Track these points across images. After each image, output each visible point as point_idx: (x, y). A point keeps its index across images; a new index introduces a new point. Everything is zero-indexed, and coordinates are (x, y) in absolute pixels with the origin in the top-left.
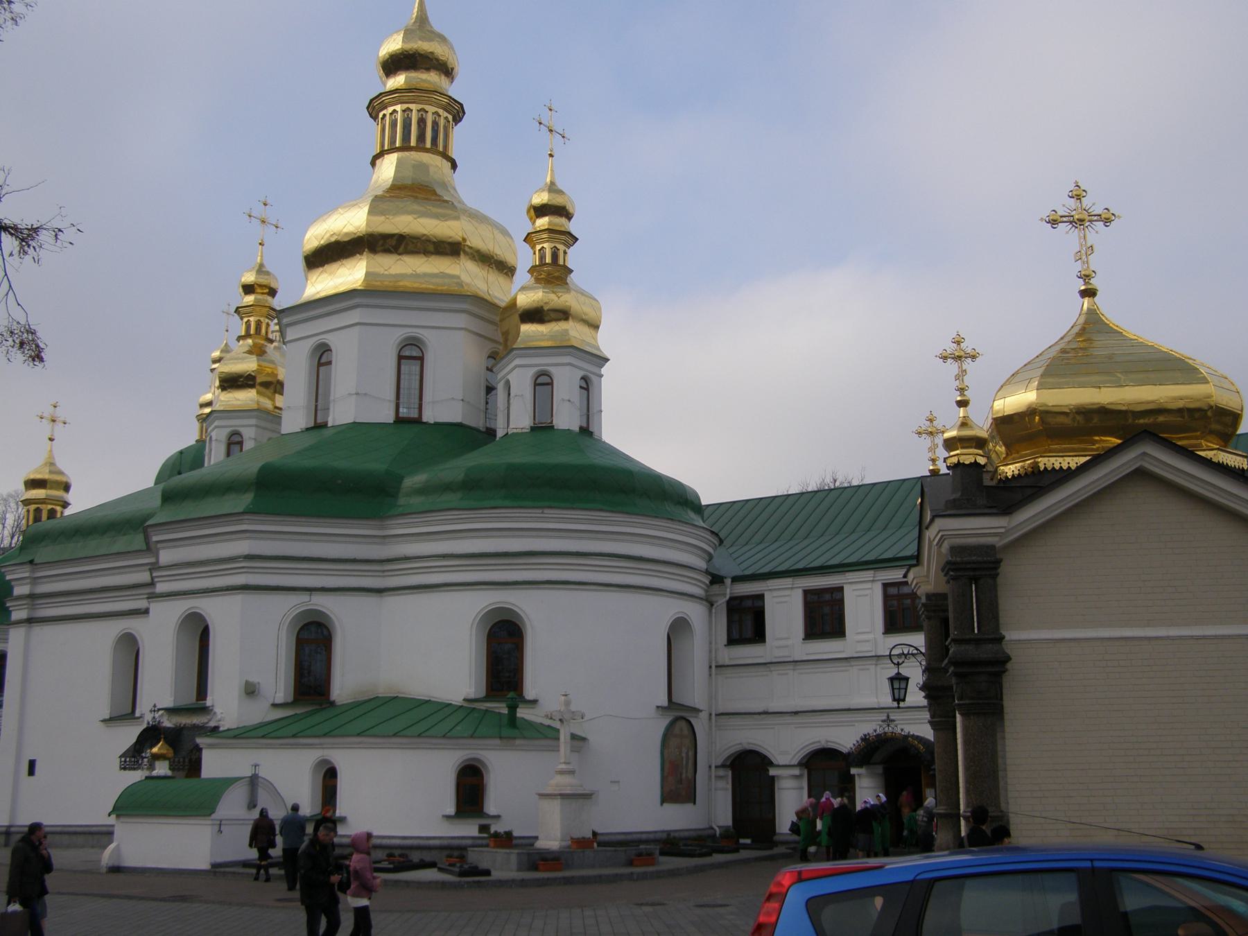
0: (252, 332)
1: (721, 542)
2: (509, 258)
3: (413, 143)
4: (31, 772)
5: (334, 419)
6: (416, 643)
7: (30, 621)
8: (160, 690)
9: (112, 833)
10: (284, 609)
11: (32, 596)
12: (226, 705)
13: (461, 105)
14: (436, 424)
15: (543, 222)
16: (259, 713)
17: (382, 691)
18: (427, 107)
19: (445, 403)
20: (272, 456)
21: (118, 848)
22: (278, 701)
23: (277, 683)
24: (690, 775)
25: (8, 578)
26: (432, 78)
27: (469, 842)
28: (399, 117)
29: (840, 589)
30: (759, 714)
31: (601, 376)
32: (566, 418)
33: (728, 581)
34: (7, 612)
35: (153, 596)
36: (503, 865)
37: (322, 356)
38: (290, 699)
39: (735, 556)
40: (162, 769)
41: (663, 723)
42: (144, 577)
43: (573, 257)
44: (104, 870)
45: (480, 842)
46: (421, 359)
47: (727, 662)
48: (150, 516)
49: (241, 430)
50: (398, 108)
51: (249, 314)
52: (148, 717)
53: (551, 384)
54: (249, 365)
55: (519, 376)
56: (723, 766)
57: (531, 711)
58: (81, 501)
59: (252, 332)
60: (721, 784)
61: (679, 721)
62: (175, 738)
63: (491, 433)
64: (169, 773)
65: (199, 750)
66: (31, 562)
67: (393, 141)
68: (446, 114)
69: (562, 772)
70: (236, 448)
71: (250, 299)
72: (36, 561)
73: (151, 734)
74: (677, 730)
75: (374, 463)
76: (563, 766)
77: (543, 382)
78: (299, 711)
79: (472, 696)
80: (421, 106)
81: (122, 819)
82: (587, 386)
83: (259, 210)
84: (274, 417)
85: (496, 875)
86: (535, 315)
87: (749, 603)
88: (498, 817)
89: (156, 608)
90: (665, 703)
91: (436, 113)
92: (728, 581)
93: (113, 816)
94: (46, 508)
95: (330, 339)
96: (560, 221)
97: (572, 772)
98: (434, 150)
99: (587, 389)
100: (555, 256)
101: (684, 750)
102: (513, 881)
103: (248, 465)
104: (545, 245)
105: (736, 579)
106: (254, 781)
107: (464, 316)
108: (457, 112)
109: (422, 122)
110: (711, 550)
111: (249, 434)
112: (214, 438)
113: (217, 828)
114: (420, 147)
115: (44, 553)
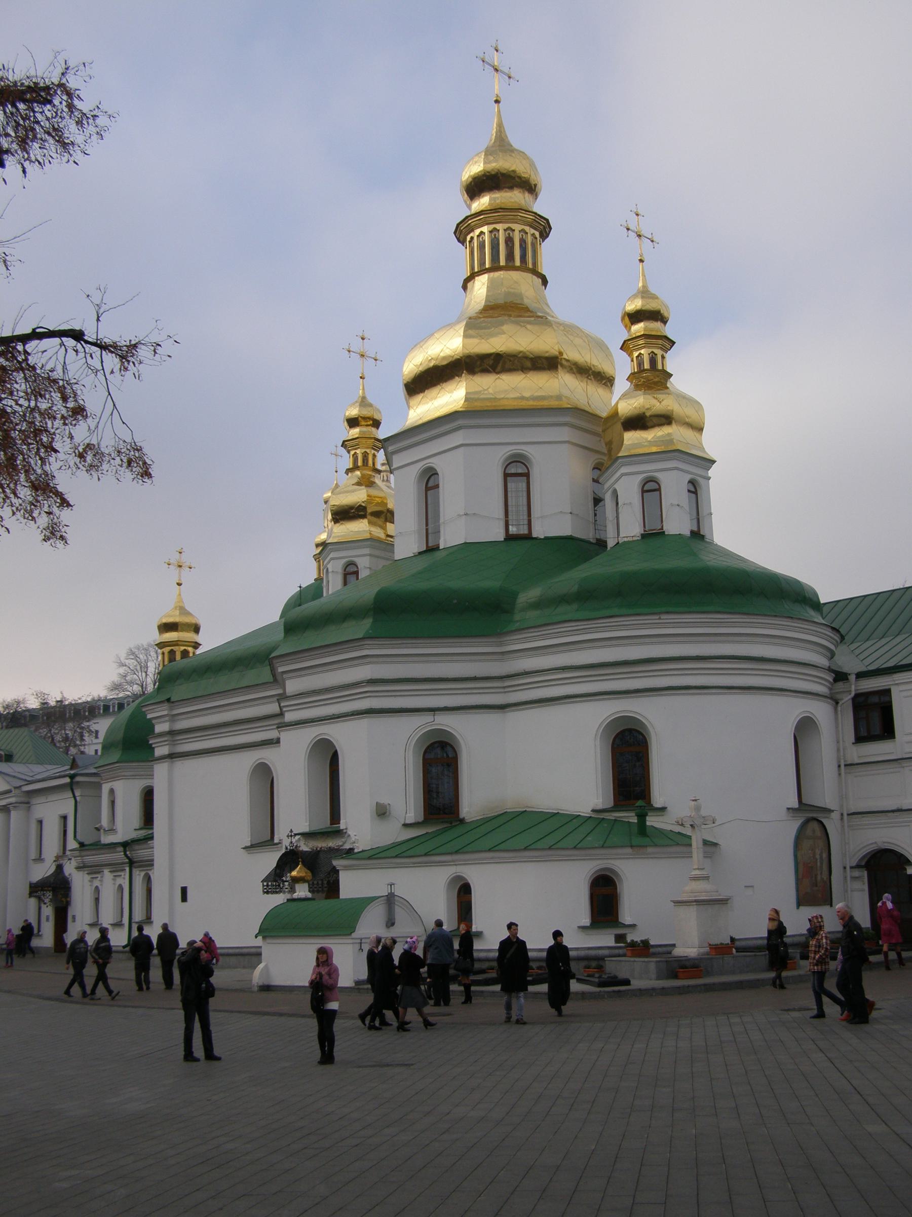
0: (360, 463)
1: (842, 638)
2: (606, 368)
3: (502, 262)
4: (184, 898)
5: (445, 541)
6: (539, 757)
7: (172, 756)
8: (295, 816)
9: (260, 954)
11: (172, 733)
12: (360, 828)
13: (547, 220)
14: (546, 538)
15: (639, 328)
16: (391, 833)
17: (511, 805)
18: (513, 226)
19: (554, 517)
20: (387, 582)
21: (266, 966)
22: (408, 822)
23: (407, 804)
24: (825, 878)
25: (149, 716)
26: (514, 197)
27: (606, 952)
28: (487, 238)
30: (893, 811)
31: (709, 478)
32: (677, 523)
33: (852, 678)
34: (151, 749)
35: (280, 726)
36: (642, 975)
37: (429, 481)
38: (421, 818)
39: (857, 652)
40: (302, 891)
41: (795, 825)
42: (273, 708)
43: (672, 362)
44: (256, 989)
45: (617, 951)
46: (527, 475)
47: (857, 761)
48: (274, 649)
50: (485, 229)
51: (355, 447)
52: (286, 842)
53: (659, 490)
54: (359, 496)
55: (626, 485)
56: (858, 866)
57: (661, 819)
58: (210, 640)
59: (360, 463)
60: (857, 885)
61: (811, 822)
62: (312, 861)
63: (601, 544)
64: (309, 895)
65: (336, 872)
66: (168, 700)
67: (482, 262)
68: (533, 231)
69: (695, 879)
70: (352, 578)
71: (355, 432)
72: (172, 700)
73: (290, 859)
74: (809, 832)
75: (487, 581)
76: (697, 872)
77: (651, 488)
78: (430, 830)
79: (600, 807)
80: (506, 226)
81: (268, 941)
82: (695, 489)
83: (357, 345)
84: (385, 546)
85: (636, 984)
86: (638, 422)
87: (875, 699)
88: (633, 926)
89: (286, 736)
90: (796, 805)
91: (523, 231)
92: (852, 678)
93: (260, 938)
94: (179, 649)
95: (436, 463)
96: (655, 327)
97: (706, 878)
98: (524, 268)
99: (695, 493)
100: (653, 361)
101: (818, 852)
102: (653, 989)
103: (365, 592)
104: (642, 351)
105: (860, 675)
106: (390, 900)
107: (566, 429)
108: (544, 228)
109: (509, 241)
110: (832, 647)
111: (364, 564)
112: (330, 570)
113: (358, 946)
114: (510, 266)
115: (180, 691)
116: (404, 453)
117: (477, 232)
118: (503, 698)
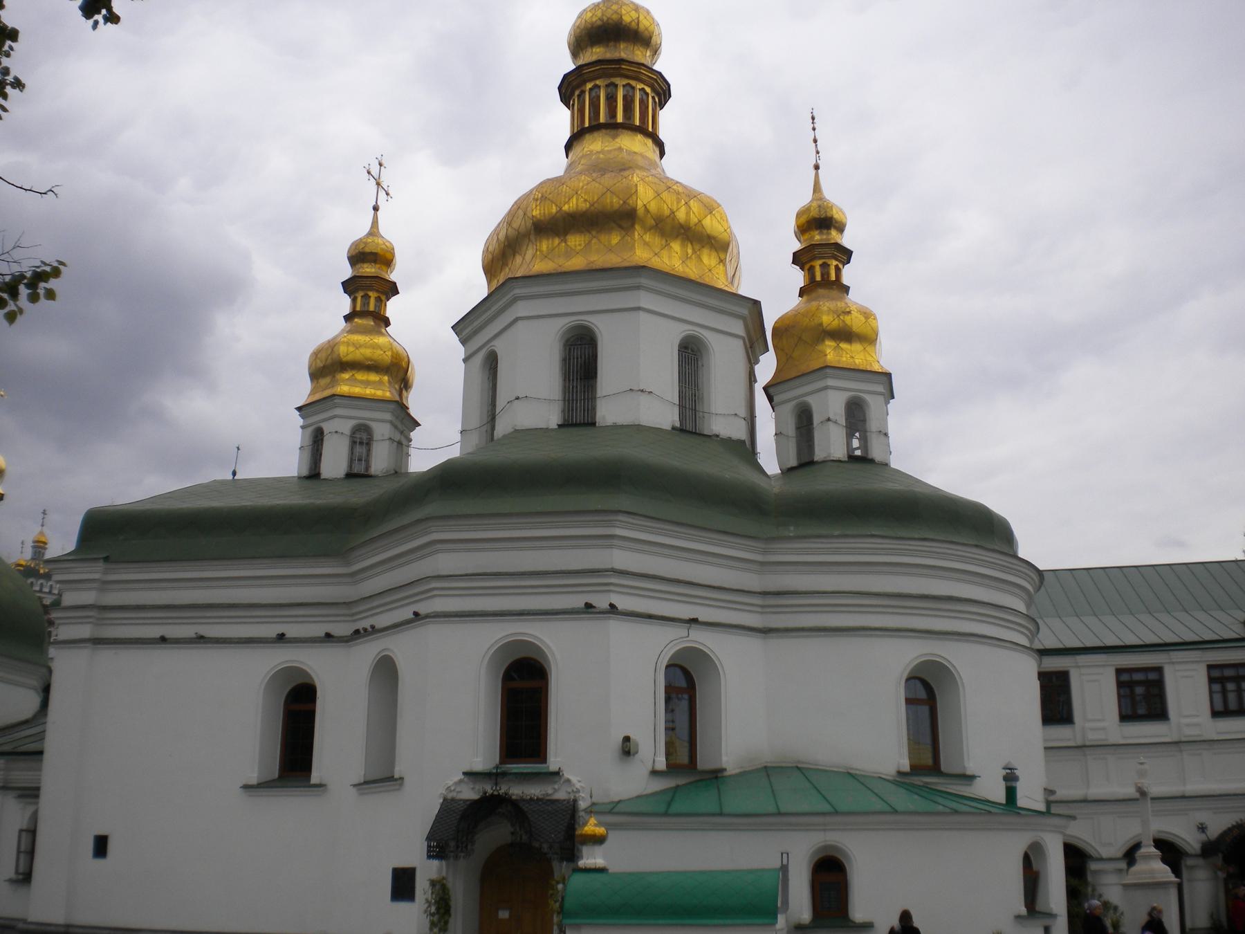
10: (661, 644)
16: (634, 782)
29: (1159, 670)
49: (373, 425)
51: (356, 290)
116: (613, 295)
117: (607, 81)
118: (777, 618)
